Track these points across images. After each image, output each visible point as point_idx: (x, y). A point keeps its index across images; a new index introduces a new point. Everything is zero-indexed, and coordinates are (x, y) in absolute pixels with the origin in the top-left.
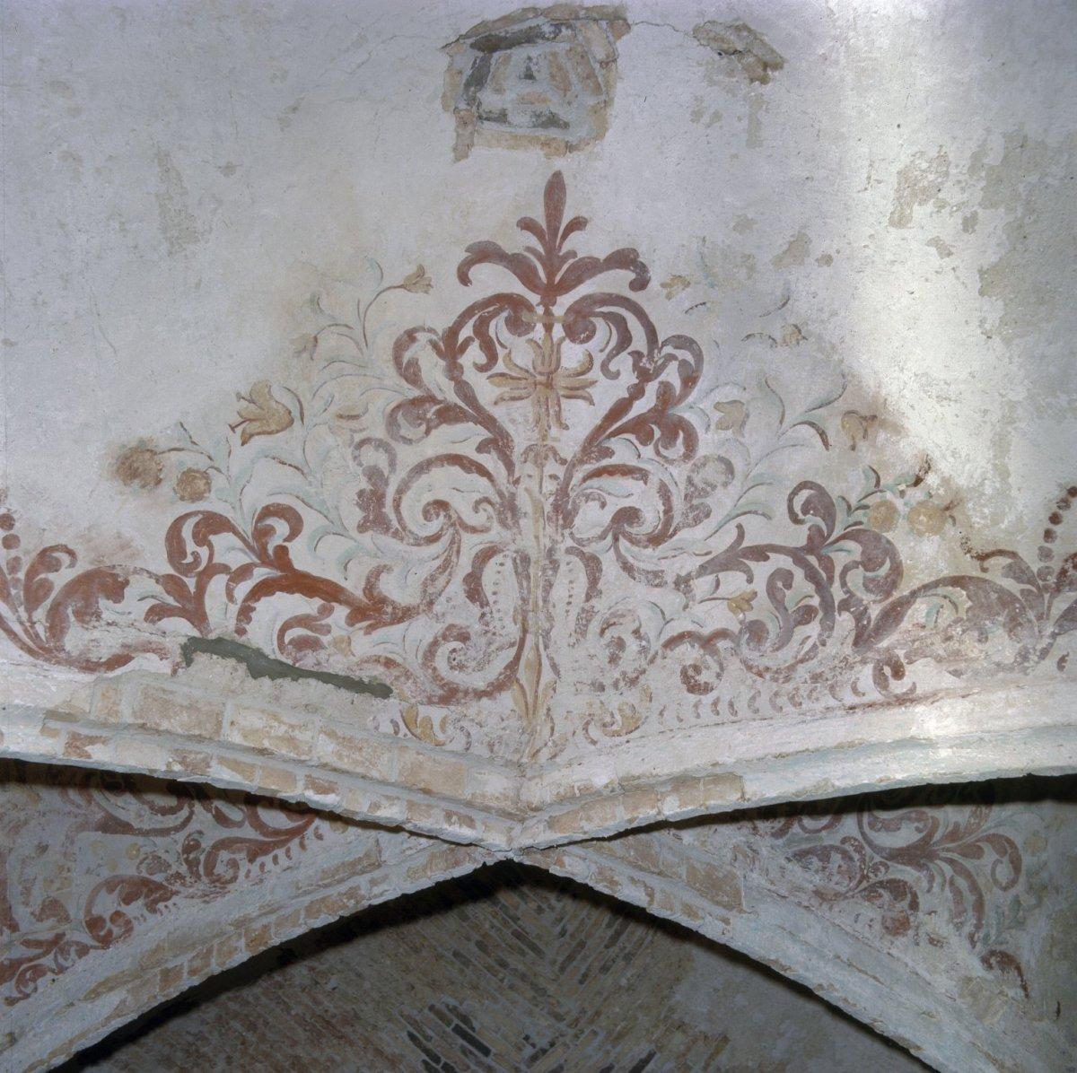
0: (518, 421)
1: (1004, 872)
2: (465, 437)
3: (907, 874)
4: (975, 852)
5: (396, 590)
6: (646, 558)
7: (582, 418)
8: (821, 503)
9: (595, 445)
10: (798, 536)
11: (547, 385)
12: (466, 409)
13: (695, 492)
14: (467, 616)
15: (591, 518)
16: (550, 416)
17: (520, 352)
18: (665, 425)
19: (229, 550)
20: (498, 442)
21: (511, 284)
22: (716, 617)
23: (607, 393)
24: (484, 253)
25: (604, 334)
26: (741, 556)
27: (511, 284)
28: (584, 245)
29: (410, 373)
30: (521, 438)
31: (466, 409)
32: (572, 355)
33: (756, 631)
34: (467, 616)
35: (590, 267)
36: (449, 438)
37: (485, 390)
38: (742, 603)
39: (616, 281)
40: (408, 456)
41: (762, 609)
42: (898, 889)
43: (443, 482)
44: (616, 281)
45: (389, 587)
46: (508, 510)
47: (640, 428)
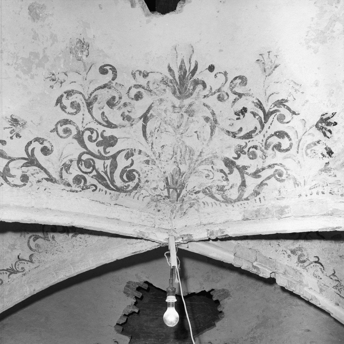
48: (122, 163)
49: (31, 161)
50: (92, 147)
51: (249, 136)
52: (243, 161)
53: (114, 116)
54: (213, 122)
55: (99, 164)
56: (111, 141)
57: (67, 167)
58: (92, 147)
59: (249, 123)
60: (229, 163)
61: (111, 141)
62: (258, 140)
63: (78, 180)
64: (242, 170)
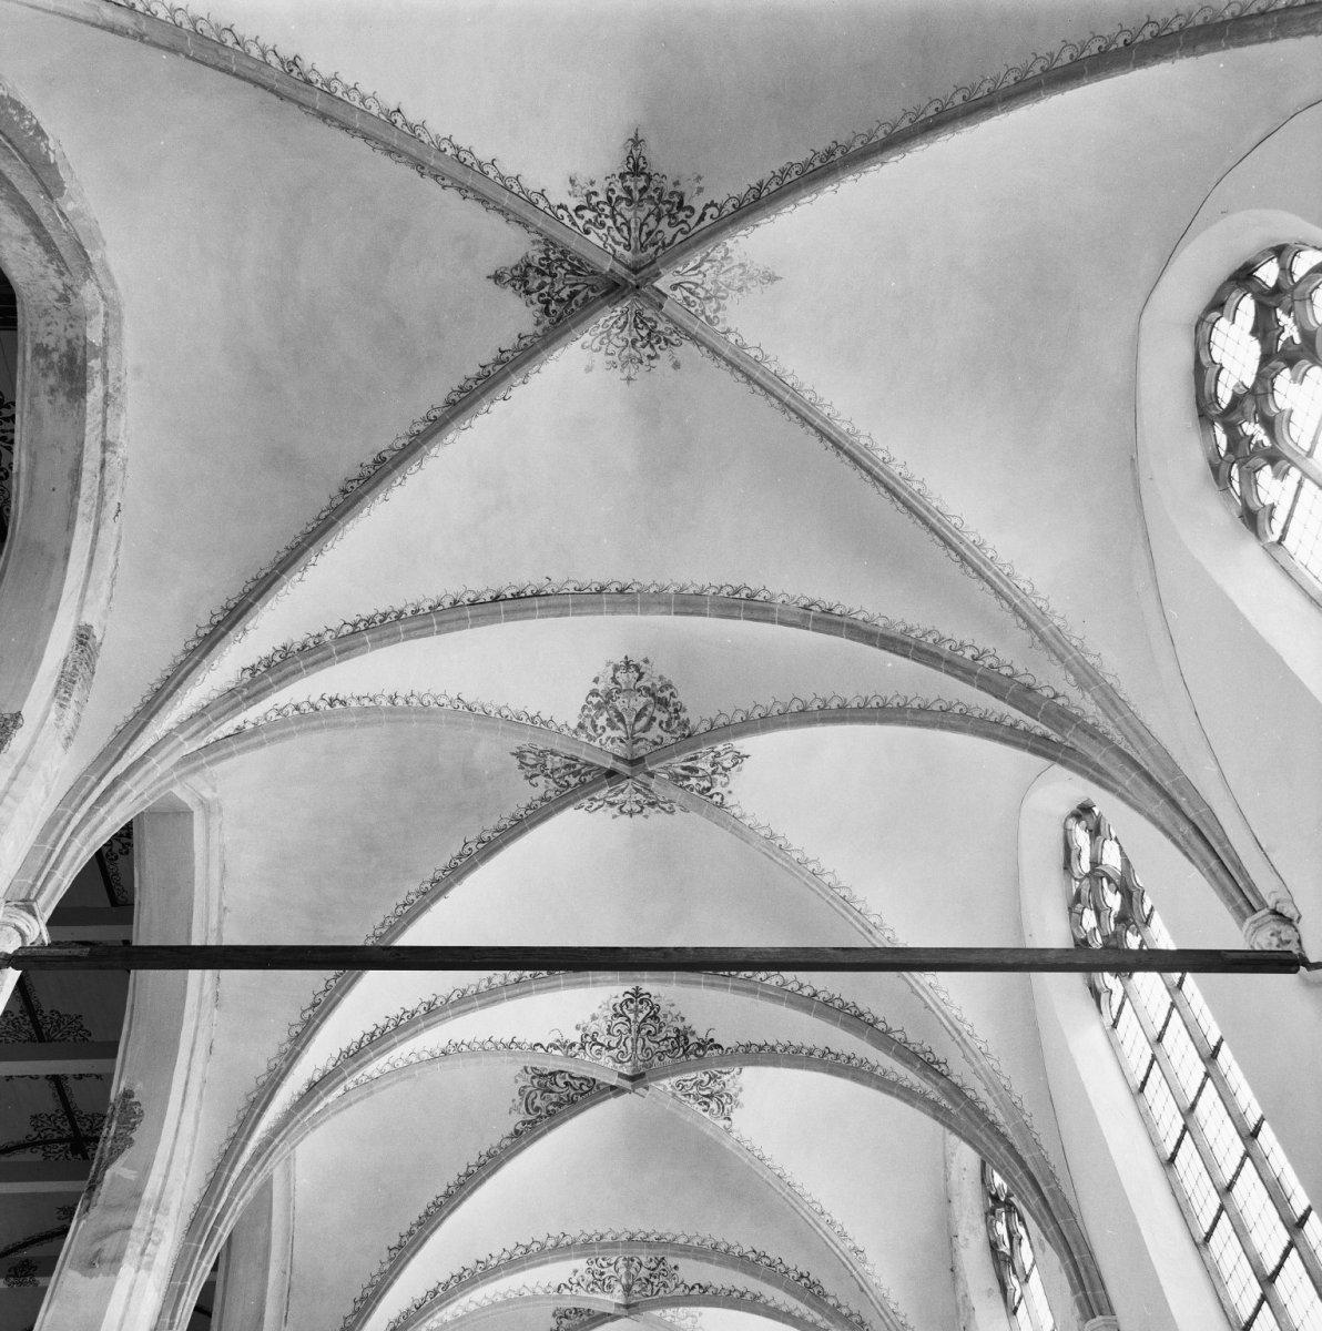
0: (632, 1016)
1: (729, 1101)
2: (623, 1019)
3: (708, 1100)
4: (722, 1096)
5: (613, 1044)
6: (653, 1038)
7: (642, 1016)
8: (678, 1030)
9: (644, 1020)
10: (675, 1035)
11: (636, 1011)
12: (623, 1015)
13: (661, 1027)
14: (623, 1049)
15: (643, 1032)
16: (637, 1016)
17: (632, 1006)
18: (655, 1017)
19: (589, 1039)
20: (629, 1020)
21: (630, 996)
22: (663, 1048)
23: (646, 1012)
24: (627, 993)
25: (645, 1003)
26: (666, 1039)
27: (630, 996)
28: (641, 992)
29: (615, 1010)
30: (632, 1019)
31: (623, 1015)
32: (640, 1007)
33: (669, 1051)
34: (623, 1049)
35: (642, 995)
36: (620, 1020)
37: (627, 1012)
38: (667, 1046)
39: (647, 997)
40: (614, 1023)
41: (670, 1047)
42: (706, 1103)
43: (620, 1027)
44: (647, 997)
45: (611, 1044)
46: (630, 1031)
47: (651, 1018)
48: (607, 1282)
49: (579, 1284)
50: (597, 1276)
51: (654, 1269)
52: (652, 1280)
53: (604, 1264)
54: (640, 1264)
55: (599, 1283)
56: (602, 1274)
57: (588, 1286)
58: (597, 1276)
59: (653, 1265)
60: (647, 1280)
61: (602, 1274)
62: (656, 1272)
63: (592, 1290)
64: (652, 1283)
